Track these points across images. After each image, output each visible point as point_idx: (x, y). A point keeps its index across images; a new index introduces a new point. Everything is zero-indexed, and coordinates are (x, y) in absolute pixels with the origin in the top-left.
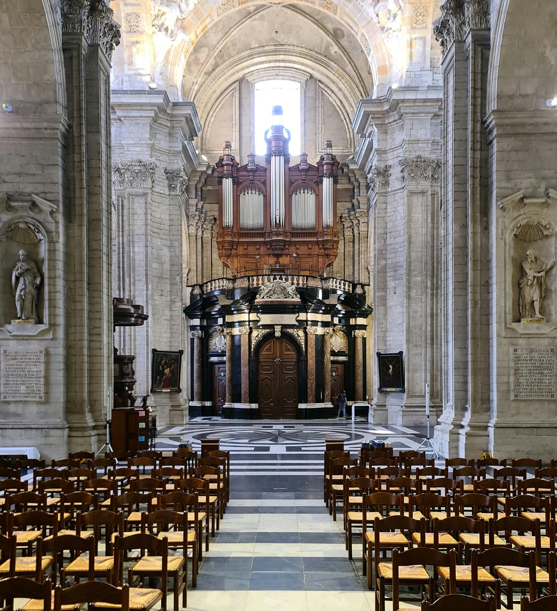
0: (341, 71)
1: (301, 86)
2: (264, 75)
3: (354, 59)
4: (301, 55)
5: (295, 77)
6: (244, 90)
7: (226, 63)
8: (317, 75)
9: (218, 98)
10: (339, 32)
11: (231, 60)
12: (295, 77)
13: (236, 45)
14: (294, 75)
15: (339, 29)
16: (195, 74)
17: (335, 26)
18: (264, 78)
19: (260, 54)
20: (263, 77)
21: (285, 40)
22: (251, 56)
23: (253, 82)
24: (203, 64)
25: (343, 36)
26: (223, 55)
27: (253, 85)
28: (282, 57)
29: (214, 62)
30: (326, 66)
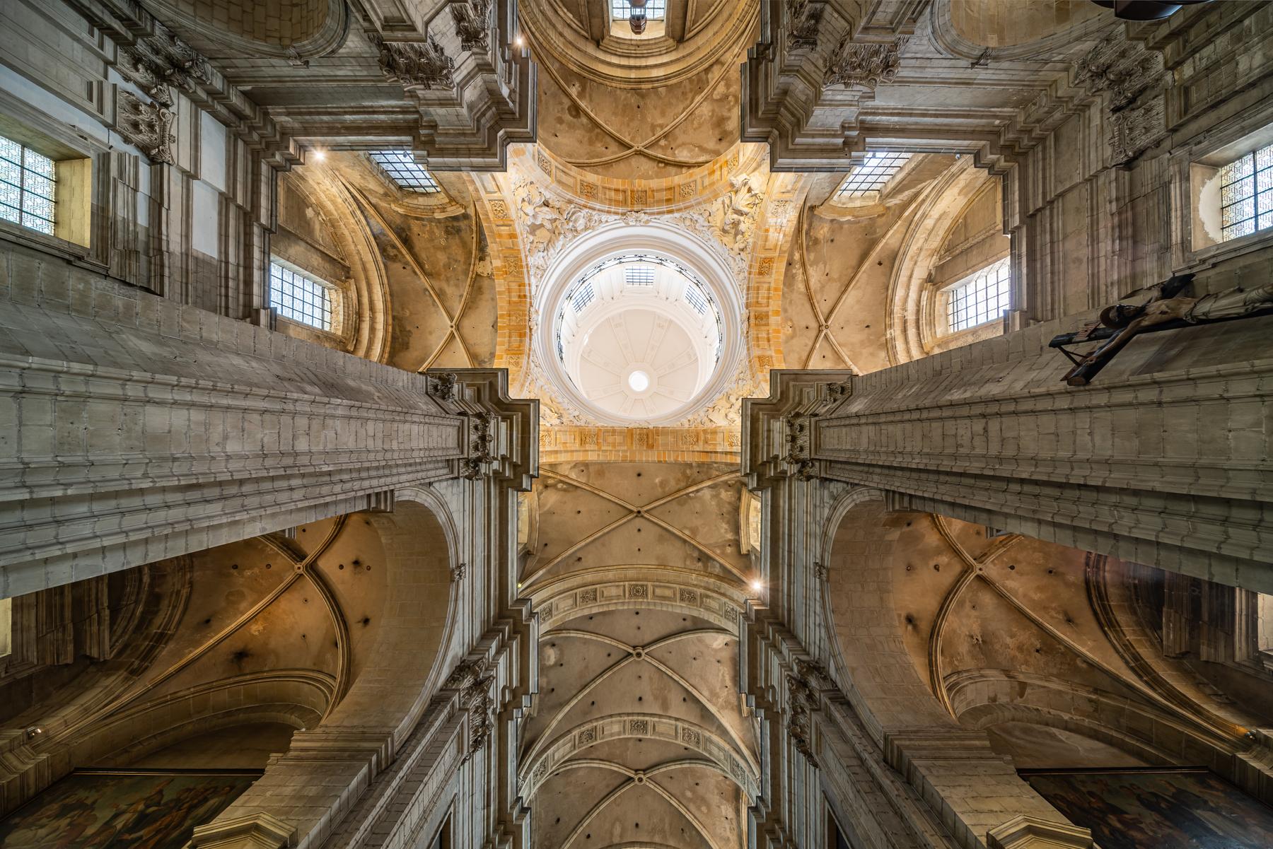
7: (695, 72)
11: (689, 75)
29: (710, 76)
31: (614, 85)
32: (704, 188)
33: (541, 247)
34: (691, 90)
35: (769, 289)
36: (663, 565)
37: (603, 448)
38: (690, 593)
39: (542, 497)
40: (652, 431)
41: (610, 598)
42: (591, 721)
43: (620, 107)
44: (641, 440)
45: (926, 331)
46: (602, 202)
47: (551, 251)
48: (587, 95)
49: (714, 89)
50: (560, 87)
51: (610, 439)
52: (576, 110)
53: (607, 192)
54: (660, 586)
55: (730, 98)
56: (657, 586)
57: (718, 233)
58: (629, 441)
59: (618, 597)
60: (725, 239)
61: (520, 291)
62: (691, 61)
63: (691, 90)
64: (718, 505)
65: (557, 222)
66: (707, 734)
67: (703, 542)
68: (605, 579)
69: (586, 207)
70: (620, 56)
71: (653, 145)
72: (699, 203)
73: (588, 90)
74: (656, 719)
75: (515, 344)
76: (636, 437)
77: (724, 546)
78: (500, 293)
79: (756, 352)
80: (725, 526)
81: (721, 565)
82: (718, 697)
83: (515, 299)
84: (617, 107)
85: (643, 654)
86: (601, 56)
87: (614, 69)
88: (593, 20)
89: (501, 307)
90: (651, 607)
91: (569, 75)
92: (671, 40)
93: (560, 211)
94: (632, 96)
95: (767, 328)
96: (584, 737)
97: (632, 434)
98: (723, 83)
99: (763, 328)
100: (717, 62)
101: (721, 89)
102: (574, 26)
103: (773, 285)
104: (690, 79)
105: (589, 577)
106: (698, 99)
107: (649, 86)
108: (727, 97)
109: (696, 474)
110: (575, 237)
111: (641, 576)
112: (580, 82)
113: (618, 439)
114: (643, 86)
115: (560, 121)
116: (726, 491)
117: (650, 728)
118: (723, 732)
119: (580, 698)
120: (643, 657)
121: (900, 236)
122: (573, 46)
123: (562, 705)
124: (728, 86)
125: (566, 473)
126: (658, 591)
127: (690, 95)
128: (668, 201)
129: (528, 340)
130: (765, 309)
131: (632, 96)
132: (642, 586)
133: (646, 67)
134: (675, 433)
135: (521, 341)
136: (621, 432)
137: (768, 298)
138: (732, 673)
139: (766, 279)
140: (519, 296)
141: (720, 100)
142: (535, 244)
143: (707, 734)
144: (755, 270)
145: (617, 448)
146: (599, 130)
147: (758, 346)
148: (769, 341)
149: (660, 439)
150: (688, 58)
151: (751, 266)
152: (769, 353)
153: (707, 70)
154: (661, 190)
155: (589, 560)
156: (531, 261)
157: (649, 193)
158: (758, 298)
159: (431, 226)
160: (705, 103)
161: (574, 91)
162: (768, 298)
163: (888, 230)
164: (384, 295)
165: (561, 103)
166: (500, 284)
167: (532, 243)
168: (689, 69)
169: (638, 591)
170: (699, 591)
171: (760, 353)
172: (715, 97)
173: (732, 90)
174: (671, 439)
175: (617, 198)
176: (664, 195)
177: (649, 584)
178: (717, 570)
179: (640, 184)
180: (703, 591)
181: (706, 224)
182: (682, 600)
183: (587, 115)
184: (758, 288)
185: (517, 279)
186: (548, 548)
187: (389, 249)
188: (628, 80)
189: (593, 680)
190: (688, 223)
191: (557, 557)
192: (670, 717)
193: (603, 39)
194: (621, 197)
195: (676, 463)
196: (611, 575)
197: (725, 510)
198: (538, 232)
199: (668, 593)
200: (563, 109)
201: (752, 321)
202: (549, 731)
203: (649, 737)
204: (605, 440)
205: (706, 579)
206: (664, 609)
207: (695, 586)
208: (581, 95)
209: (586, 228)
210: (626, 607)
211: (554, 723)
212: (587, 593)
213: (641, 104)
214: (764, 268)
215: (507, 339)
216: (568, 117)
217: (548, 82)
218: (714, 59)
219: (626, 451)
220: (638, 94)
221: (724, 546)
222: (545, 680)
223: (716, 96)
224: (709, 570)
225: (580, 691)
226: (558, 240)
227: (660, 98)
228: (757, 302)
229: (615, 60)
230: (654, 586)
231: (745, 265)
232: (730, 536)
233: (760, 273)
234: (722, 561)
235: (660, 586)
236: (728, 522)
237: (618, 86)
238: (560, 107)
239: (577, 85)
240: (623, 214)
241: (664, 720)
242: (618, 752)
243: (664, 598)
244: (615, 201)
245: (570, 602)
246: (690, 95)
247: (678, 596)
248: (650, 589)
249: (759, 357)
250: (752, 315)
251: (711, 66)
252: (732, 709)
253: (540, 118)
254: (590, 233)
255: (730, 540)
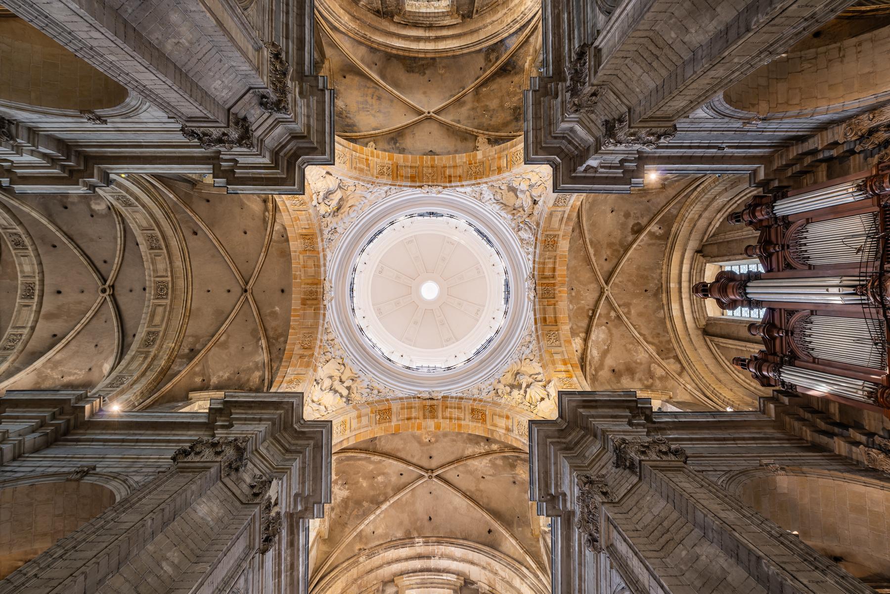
0: (678, 218)
1: (709, 262)
2: (699, 305)
3: (659, 208)
4: (669, 265)
5: (701, 270)
6: (716, 330)
7: (676, 346)
8: (693, 245)
9: (720, 364)
10: (635, 228)
11: (673, 340)
12: (701, 270)
13: (659, 334)
14: (698, 271)
15: (632, 229)
16: (676, 384)
17: (630, 234)
18: (703, 305)
19: (670, 309)
20: (702, 307)
21: (656, 281)
22: (671, 318)
23: (707, 319)
24: (667, 373)
25: (638, 224)
26: (666, 349)
27: (710, 319)
28: (673, 285)
29: (672, 360)
30: (676, 236)
31: (664, 267)
32: (552, 354)
33: (498, 197)
34: (661, 342)
35: (459, 419)
36: (189, 314)
37: (301, 257)
38: (154, 341)
39: (255, 197)
40: (318, 304)
41: (153, 263)
42: (34, 243)
43: (646, 273)
44: (311, 292)
45: (416, 579)
46: (541, 255)
47: (498, 207)
48: (653, 241)
49: (659, 365)
50: (655, 215)
51: (310, 263)
52: (638, 230)
53: (552, 260)
54: (165, 312)
55: (651, 381)
56: (165, 308)
57: (516, 369)
58: (310, 281)
59: (155, 271)
60: (509, 375)
61: (455, 177)
62: (685, 342)
63: (661, 342)
64: (249, 369)
65: (522, 212)
66: (11, 359)
67: (211, 353)
68: (174, 258)
69: (536, 240)
70: (690, 273)
71: (611, 307)
72: (540, 350)
73: (658, 242)
74: (34, 308)
75: (403, 172)
76: (314, 288)
77: (203, 375)
78: (454, 158)
79: (395, 406)
80: (226, 375)
81: (180, 372)
82: (52, 369)
83: (447, 173)
84: (645, 270)
85: (104, 295)
86: (688, 255)
87: (678, 268)
88: (716, 246)
89: (442, 160)
90: (146, 303)
91: (668, 223)
92: (704, 323)
93: (530, 215)
94: (656, 284)
95: (421, 417)
96: (16, 237)
97: (316, 284)
98: (664, 373)
99: (421, 413)
100: (683, 368)
101: (659, 372)
102: (710, 229)
103: (463, 422)
104: (669, 341)
105: (174, 243)
106: (651, 349)
107: (665, 302)
108: (652, 377)
109: (278, 347)
110: (513, 229)
111: (178, 293)
112: (665, 232)
113: (311, 271)
114: (664, 295)
115: (627, 215)
116: (260, 377)
117: (27, 301)
118: (9, 374)
119: (57, 233)
120: (102, 295)
121: (511, 552)
122: (694, 227)
123: (50, 217)
124: (661, 378)
125: (277, 220)
126: (160, 310)
127: (656, 341)
128: (545, 319)
129: (409, 184)
130: (440, 415)
131: (656, 284)
132: (167, 294)
133: (681, 298)
134: (315, 326)
135: (407, 177)
136: (318, 273)
137: (451, 418)
138: (76, 383)
139: (469, 416)
140: (450, 176)
141: (650, 371)
142: (499, 191)
143: (11, 359)
144: (476, 405)
145: (302, 270)
146: (622, 252)
147: (402, 409)
148: (408, 419)
149: (310, 311)
150: (688, 339)
151: (481, 401)
152: (394, 418)
153: (676, 358)
154: (555, 313)
155: (193, 242)
156: (484, 187)
157: (552, 301)
158: (451, 408)
159: (520, 93)
160: (647, 356)
161: (654, 228)
162: (451, 418)
163: (516, 539)
164: (451, 50)
165: (642, 216)
166: (462, 158)
167: (500, 188)
168: (678, 341)
169: (161, 290)
170: (153, 351)
171: (394, 410)
172: (653, 365)
173: (658, 382)
174: (310, 322)
175: (547, 270)
176: (550, 315)
177: (168, 301)
178: (175, 368)
179: (563, 293)
180: (152, 354)
181: (524, 357)
182: (149, 333)
183: (634, 241)
184: (459, 408)
185: (465, 174)
186: (204, 203)
187: (495, 54)
188: (668, 281)
189: (78, 246)
190: (528, 339)
191: (193, 211)
192: (36, 321)
193: (703, 256)
194: (547, 273)
195: (288, 326)
196: (178, 263)
197: (242, 376)
198: (512, 194)
199: (157, 319)
200: (638, 218)
201: (429, 403)
202: (16, 205)
203: (18, 300)
204: (309, 257)
205: (166, 357)
206: (144, 316)
207: (161, 346)
208: (652, 235)
209: (522, 240)
210: (147, 278)
211: (26, 209)
212: (157, 240)
213: (649, 294)
214: (478, 414)
215: (409, 164)
216: (631, 222)
217: (658, 204)
218: (685, 365)
219: (301, 279)
220: (657, 290)
221: (203, 375)
222: (76, 200)
223: (654, 366)
224: (178, 360)
225: (65, 234)
226: (507, 213)
227: (655, 312)
228: (447, 407)
229: (686, 268)
230: (165, 306)
231: (484, 396)
232: (214, 380)
233: (473, 410)
234: (183, 373)
235: (165, 312)
236: (229, 379)
237: (664, 271)
238: (638, 215)
239: (661, 232)
240: (533, 275)
241: (33, 315)
242: (9, 270)
243: (153, 316)
244: (544, 268)
245: (145, 224)
246: (656, 341)
247: (153, 329)
248: (163, 302)
249: (390, 409)
250: (435, 402)
251: (680, 362)
252: (37, 383)
253: (626, 196)
254: (518, 243)
255: (210, 380)
